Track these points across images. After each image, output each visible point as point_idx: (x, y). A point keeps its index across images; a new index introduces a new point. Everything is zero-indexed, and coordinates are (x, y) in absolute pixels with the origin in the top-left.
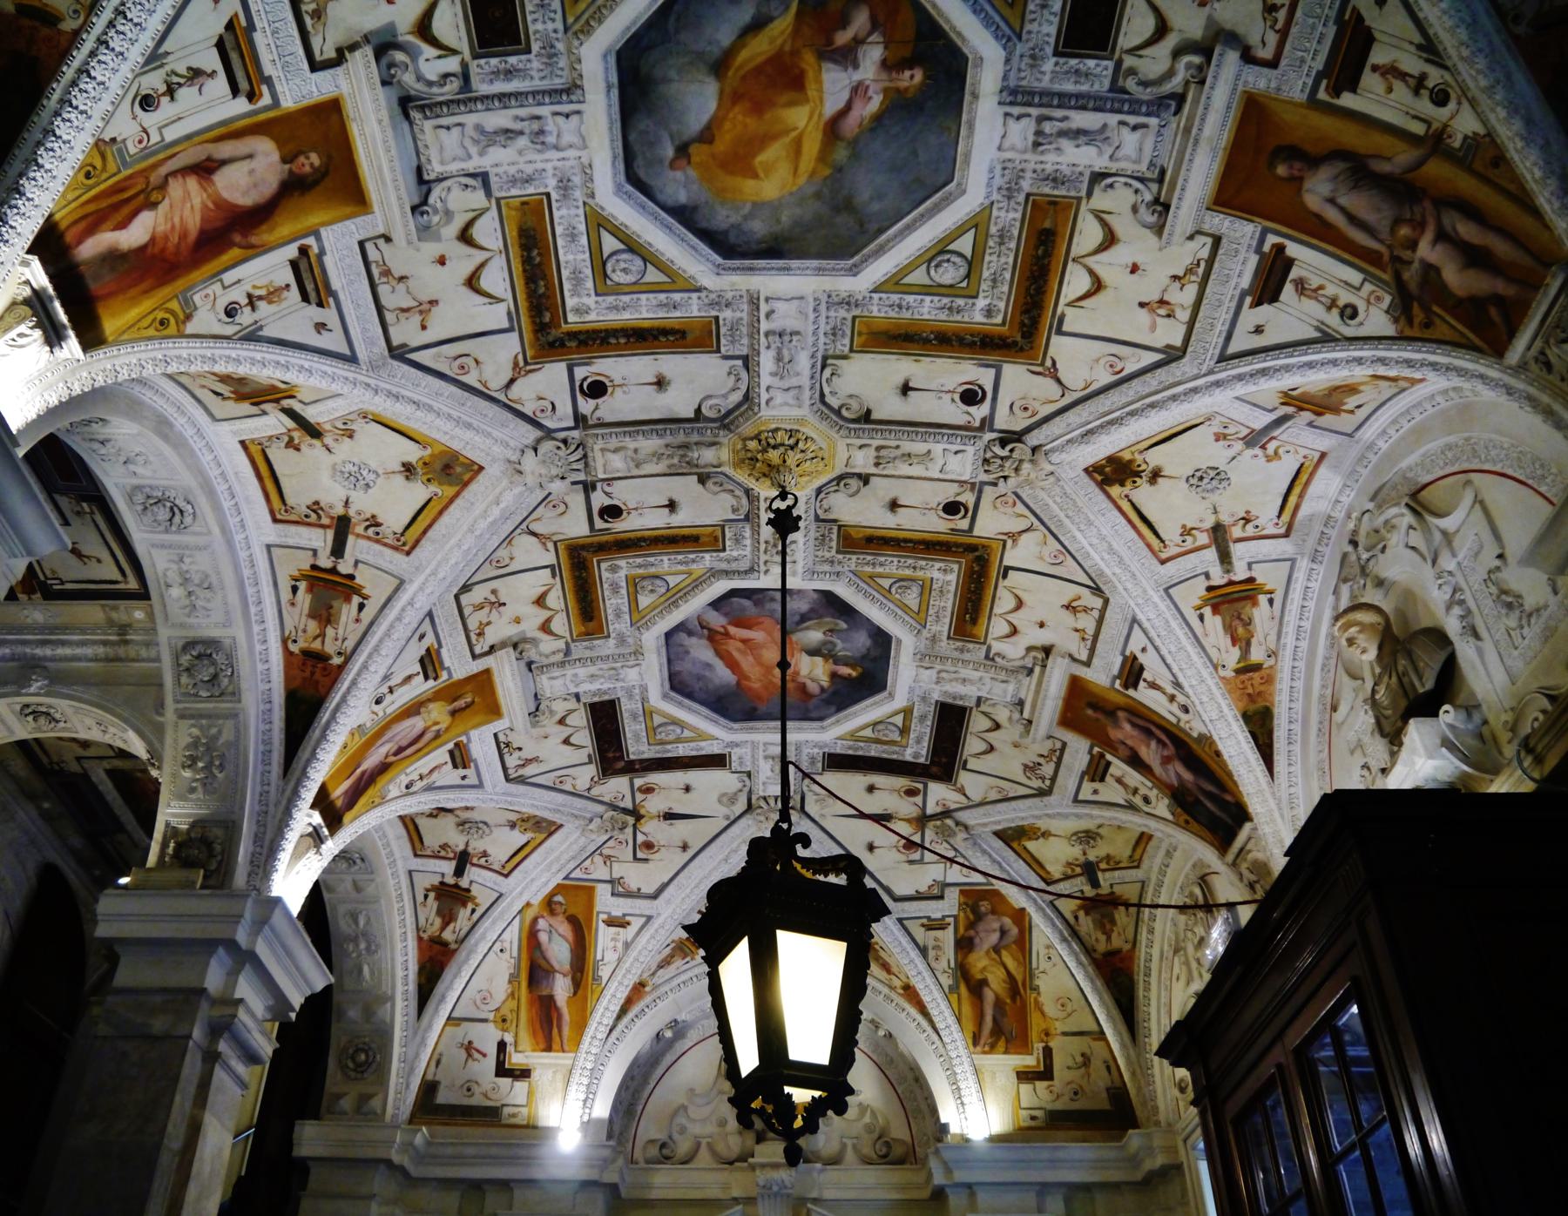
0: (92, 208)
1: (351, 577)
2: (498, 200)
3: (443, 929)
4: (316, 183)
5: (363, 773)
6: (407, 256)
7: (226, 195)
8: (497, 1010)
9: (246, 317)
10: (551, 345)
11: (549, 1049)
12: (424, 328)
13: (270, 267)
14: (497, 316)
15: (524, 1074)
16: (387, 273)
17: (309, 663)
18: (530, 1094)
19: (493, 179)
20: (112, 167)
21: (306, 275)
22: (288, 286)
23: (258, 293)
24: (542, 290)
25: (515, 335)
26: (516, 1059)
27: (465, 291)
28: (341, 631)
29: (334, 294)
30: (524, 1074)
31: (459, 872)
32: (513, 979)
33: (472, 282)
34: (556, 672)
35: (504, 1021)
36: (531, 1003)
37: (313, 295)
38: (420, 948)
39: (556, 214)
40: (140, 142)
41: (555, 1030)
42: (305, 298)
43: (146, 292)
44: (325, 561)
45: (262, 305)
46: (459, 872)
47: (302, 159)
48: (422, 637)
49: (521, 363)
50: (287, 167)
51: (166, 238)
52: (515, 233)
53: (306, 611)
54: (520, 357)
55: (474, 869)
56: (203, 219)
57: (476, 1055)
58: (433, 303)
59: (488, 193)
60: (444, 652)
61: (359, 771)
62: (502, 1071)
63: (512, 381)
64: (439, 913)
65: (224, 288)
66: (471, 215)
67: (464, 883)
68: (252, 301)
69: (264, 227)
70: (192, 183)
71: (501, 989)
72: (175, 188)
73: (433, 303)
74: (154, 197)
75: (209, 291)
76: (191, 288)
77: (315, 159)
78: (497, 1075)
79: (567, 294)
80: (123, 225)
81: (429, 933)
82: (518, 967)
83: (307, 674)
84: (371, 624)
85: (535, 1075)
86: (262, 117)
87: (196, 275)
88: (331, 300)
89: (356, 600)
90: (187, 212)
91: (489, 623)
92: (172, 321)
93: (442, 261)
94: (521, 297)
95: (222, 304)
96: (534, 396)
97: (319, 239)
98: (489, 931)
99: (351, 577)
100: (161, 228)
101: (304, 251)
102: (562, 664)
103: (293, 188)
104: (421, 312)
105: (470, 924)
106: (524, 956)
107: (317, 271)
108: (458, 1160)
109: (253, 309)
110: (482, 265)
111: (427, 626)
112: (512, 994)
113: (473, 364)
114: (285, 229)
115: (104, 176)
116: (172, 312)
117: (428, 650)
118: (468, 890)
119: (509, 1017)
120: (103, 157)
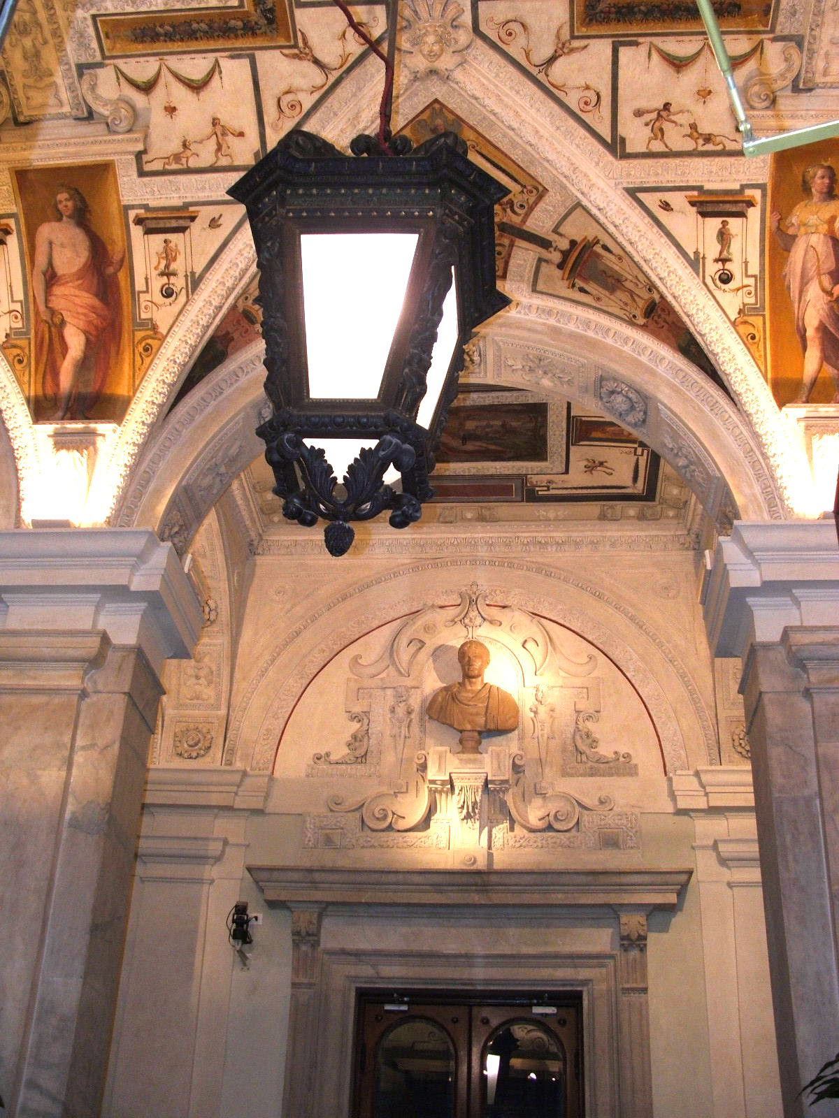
0: (42, 367)
1: (573, 243)
2: (104, 57)
4: (83, 200)
5: (822, 328)
6: (164, 141)
7: (75, 269)
9: (178, 283)
10: (271, 22)
12: (241, 134)
13: (145, 252)
14: (235, 71)
16: (177, 158)
17: (656, 318)
19: (83, 60)
20: (23, 343)
21: (161, 225)
22: (165, 241)
23: (162, 266)
24: (203, 26)
25: (258, 54)
27: (205, 94)
28: (630, 277)
29: (186, 206)
33: (196, 87)
34: (820, 64)
37: (182, 223)
39: (112, 11)
40: (16, 318)
42: (182, 230)
43: (118, 353)
44: (556, 257)
45: (173, 266)
47: (60, 207)
48: (666, 206)
49: (296, 51)
50: (64, 218)
51: (90, 322)
52: (140, 46)
53: (607, 293)
54: (286, 51)
56: (88, 291)
58: (215, 122)
59: (100, 65)
60: (708, 186)
61: (810, 333)
63: (316, 62)
65: (147, 291)
66: (122, 80)
68: (167, 273)
69: (109, 248)
70: (58, 290)
72: (57, 303)
73: (215, 122)
74: (57, 321)
75: (143, 305)
76: (134, 319)
77: (62, 196)
79: (203, 5)
80: (65, 349)
83: (666, 326)
84: (625, 252)
86: (23, 229)
87: (126, 309)
88: (191, 209)
89: (598, 249)
90: (77, 301)
91: (693, 127)
92: (149, 341)
93: (171, 110)
94: (212, 45)
95: (158, 298)
96: (340, 42)
97: (133, 207)
99: (573, 243)
100: (82, 324)
101: (139, 221)
102: (812, 53)
103: (82, 217)
104: (224, 134)
107: (160, 215)
109: (174, 274)
110: (177, 76)
111: (651, 200)
113: (289, 97)
114: (117, 232)
115: (27, 351)
116: (144, 338)
117: (693, 204)
120: (15, 346)
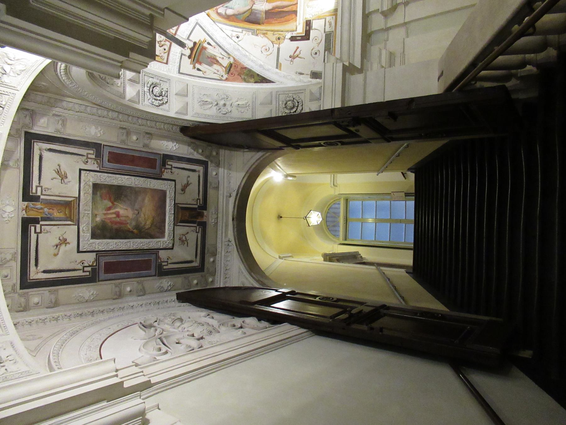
3: (221, 65)
8: (272, 42)
11: (295, 12)
15: (308, 24)
18: (319, 18)
26: (300, 30)
30: (308, 24)
31: (181, 44)
32: (255, 33)
35: (279, 39)
36: (269, 23)
38: (234, 80)
41: (285, 9)
46: (181, 44)
55: (178, 33)
57: (297, 53)
62: (306, 37)
64: (210, 64)
67: (191, 45)
71: (261, 40)
78: (308, 39)
81: (223, 74)
82: (248, 29)
85: (309, 17)
98: (219, 36)
105: (218, 47)
106: (241, 25)
108: (351, 42)
112: (264, 34)
118: (195, 43)
119: (277, 36)
